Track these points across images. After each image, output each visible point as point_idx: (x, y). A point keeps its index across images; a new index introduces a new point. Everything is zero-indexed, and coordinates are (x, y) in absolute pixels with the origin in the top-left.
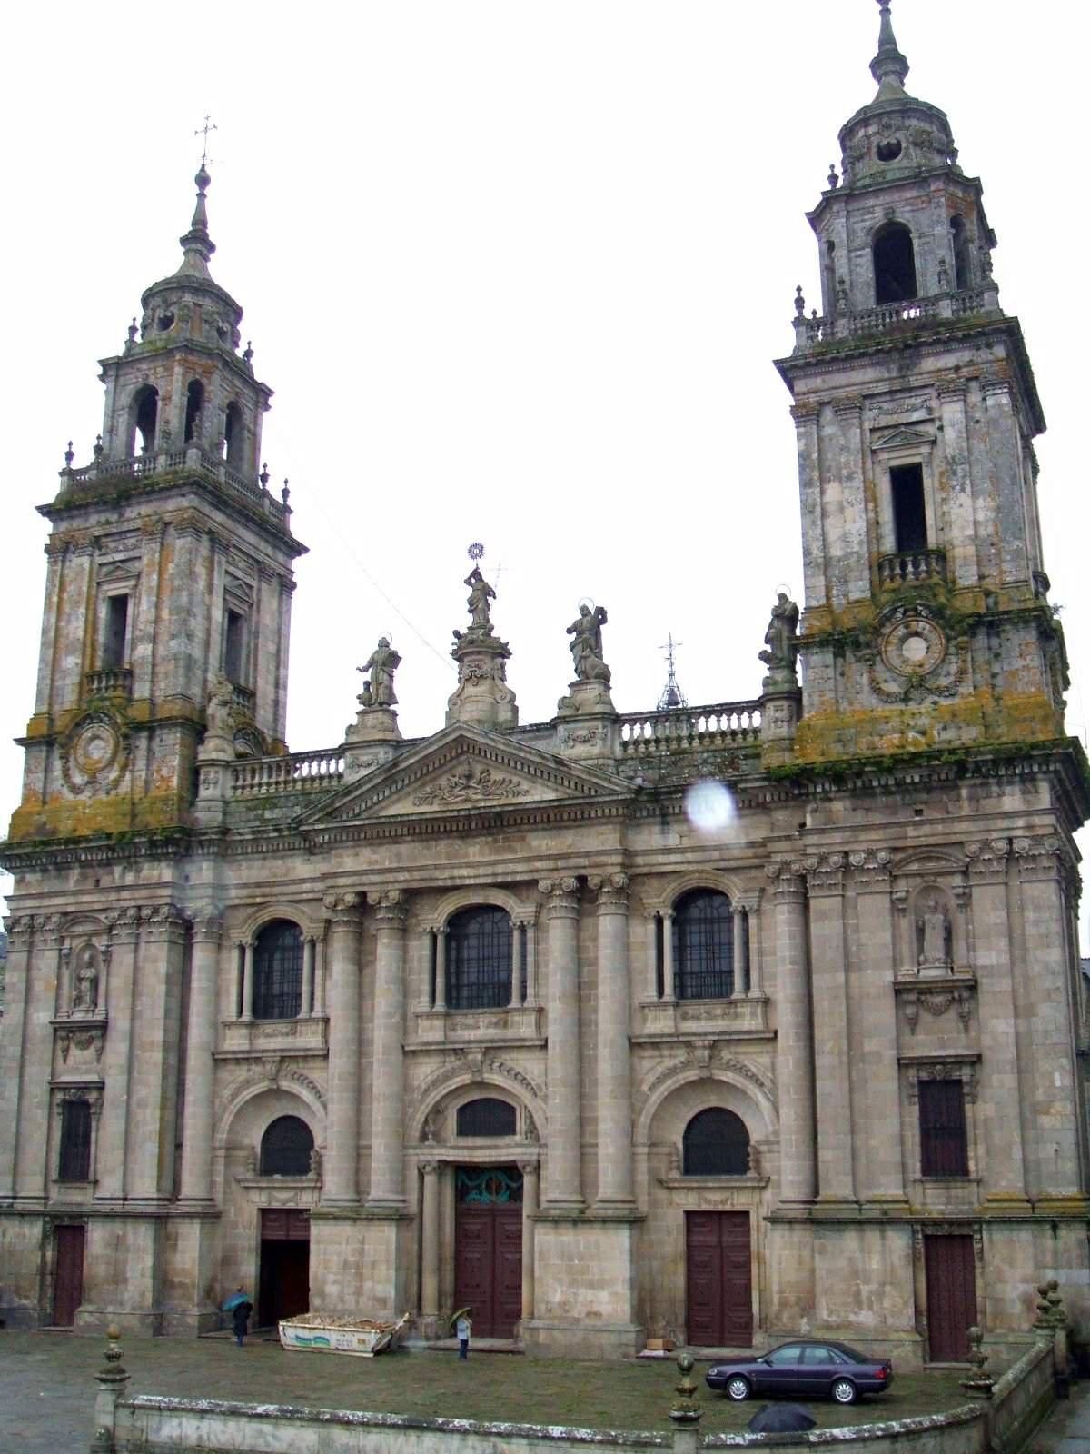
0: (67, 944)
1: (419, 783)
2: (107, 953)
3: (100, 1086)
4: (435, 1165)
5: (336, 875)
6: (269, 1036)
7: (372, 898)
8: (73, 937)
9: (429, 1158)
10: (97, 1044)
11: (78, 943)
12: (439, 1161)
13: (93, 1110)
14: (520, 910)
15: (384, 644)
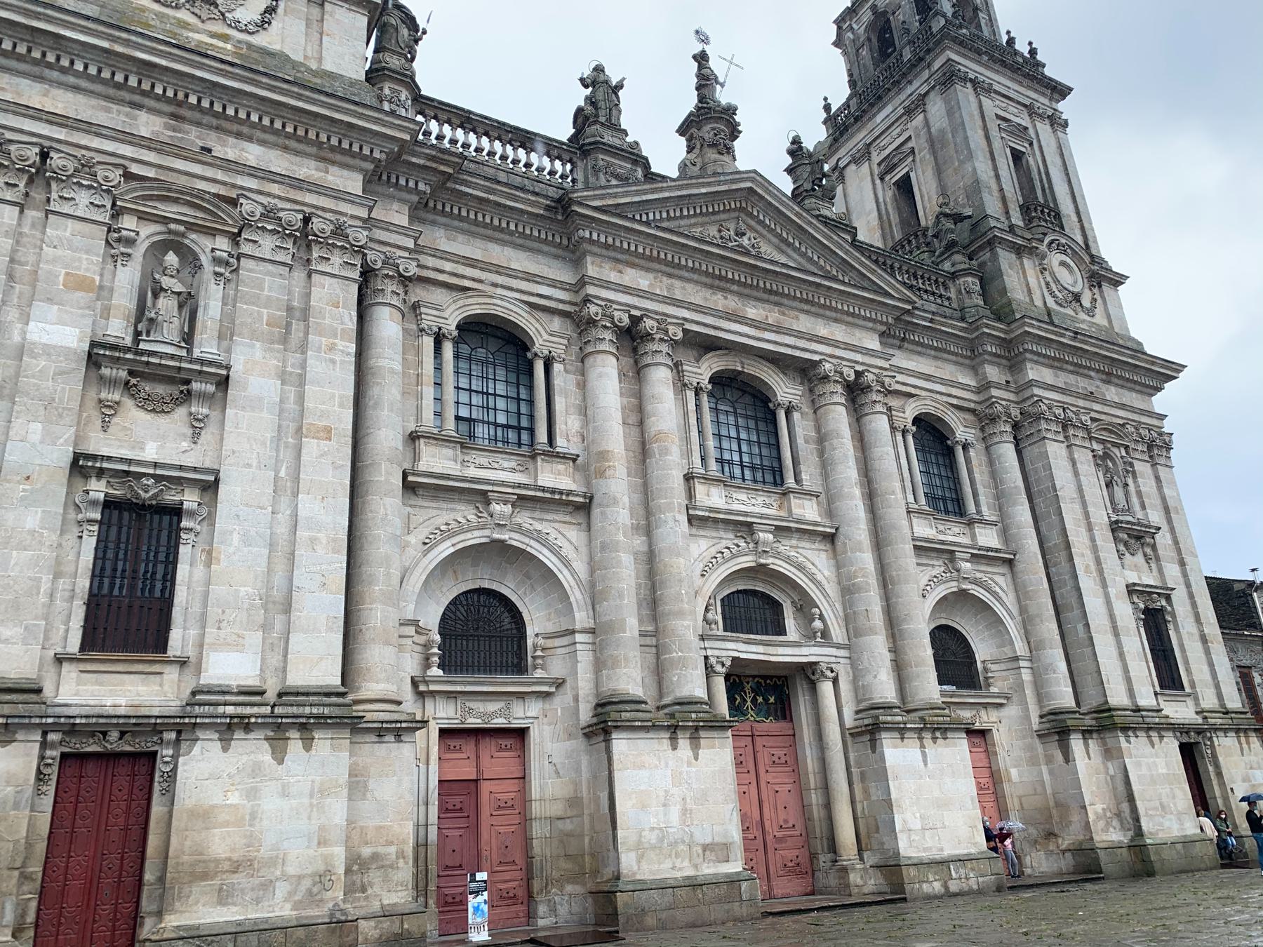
0: (128, 222)
1: (693, 221)
2: (229, 266)
3: (210, 487)
4: (728, 663)
5: (606, 285)
6: (481, 467)
7: (649, 324)
8: (143, 217)
9: (717, 653)
10: (202, 410)
11: (147, 233)
12: (734, 659)
13: (184, 524)
14: (785, 390)
15: (599, 69)
